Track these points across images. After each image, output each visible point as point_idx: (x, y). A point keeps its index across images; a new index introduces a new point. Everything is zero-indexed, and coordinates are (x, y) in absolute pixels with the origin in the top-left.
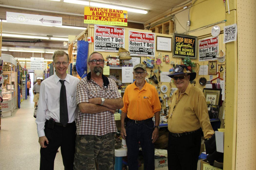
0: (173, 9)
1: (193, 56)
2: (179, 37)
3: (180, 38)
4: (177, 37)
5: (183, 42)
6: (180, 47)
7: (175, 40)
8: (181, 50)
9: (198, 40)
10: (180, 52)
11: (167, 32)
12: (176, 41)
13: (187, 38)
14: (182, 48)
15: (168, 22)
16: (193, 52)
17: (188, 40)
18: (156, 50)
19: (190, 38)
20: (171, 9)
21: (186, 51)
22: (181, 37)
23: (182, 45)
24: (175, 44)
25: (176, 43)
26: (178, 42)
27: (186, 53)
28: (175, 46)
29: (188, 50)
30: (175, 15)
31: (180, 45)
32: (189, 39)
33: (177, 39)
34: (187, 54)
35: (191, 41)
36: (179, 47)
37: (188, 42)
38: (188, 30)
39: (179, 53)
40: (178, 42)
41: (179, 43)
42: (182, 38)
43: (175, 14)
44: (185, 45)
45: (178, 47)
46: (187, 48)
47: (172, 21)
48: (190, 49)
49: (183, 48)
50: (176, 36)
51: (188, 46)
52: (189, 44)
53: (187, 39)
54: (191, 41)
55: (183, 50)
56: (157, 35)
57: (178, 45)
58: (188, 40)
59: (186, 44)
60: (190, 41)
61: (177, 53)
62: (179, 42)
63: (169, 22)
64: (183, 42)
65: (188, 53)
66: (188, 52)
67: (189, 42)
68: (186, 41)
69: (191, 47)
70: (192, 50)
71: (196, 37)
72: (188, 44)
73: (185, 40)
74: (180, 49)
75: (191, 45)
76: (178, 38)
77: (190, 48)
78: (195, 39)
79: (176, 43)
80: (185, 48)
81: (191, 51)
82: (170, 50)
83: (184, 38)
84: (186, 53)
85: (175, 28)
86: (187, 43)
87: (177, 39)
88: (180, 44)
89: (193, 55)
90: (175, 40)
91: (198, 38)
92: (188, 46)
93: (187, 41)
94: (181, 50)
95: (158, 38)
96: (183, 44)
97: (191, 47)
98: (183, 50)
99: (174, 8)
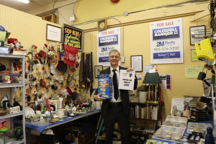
0: (56, 3)
1: (79, 49)
2: (68, 28)
3: (69, 29)
4: (66, 28)
5: (72, 33)
6: (69, 39)
7: (65, 31)
8: (70, 42)
9: (84, 34)
10: (69, 43)
11: (56, 22)
12: (65, 32)
13: (74, 30)
14: (70, 39)
15: (50, 15)
16: (79, 44)
17: (76, 32)
18: (45, 39)
19: (78, 31)
20: (53, 3)
21: (74, 43)
22: (70, 29)
23: (70, 37)
24: (64, 34)
25: (65, 34)
26: (66, 33)
27: (74, 45)
28: (64, 37)
29: (76, 42)
30: (59, 9)
31: (68, 37)
32: (77, 32)
33: (66, 30)
34: (75, 46)
35: (78, 34)
36: (68, 39)
37: (75, 34)
38: (72, 24)
39: (68, 44)
40: (66, 33)
41: (68, 34)
42: (71, 30)
43: (59, 8)
44: (73, 37)
45: (67, 38)
46: (74, 40)
47: (54, 14)
48: (77, 42)
49: (71, 40)
50: (65, 27)
51: (75, 38)
52: (76, 37)
53: (75, 31)
54: (78, 34)
55: (71, 41)
56: (48, 24)
57: (67, 36)
58: (76, 32)
59: (74, 36)
60: (77, 33)
61: (66, 44)
62: (68, 33)
63: (51, 15)
64: (72, 33)
65: (75, 45)
66: (75, 44)
67: (76, 34)
68: (74, 32)
69: (78, 39)
70: (79, 42)
71: (83, 30)
72: (75, 36)
73: (73, 32)
74: (68, 41)
75: (78, 37)
76: (67, 29)
77: (77, 41)
78: (81, 32)
79: (65, 34)
80: (73, 40)
81: (78, 44)
82: (60, 41)
83: (72, 30)
84: (74, 45)
85: (58, 21)
86: (75, 35)
87: (66, 30)
88: (69, 36)
89: (80, 47)
90: (65, 31)
91: (85, 31)
92: (75, 38)
93: (75, 33)
94: (70, 42)
95: (48, 26)
96: (71, 36)
97: (78, 39)
98: (71, 41)
99: (57, 2)
